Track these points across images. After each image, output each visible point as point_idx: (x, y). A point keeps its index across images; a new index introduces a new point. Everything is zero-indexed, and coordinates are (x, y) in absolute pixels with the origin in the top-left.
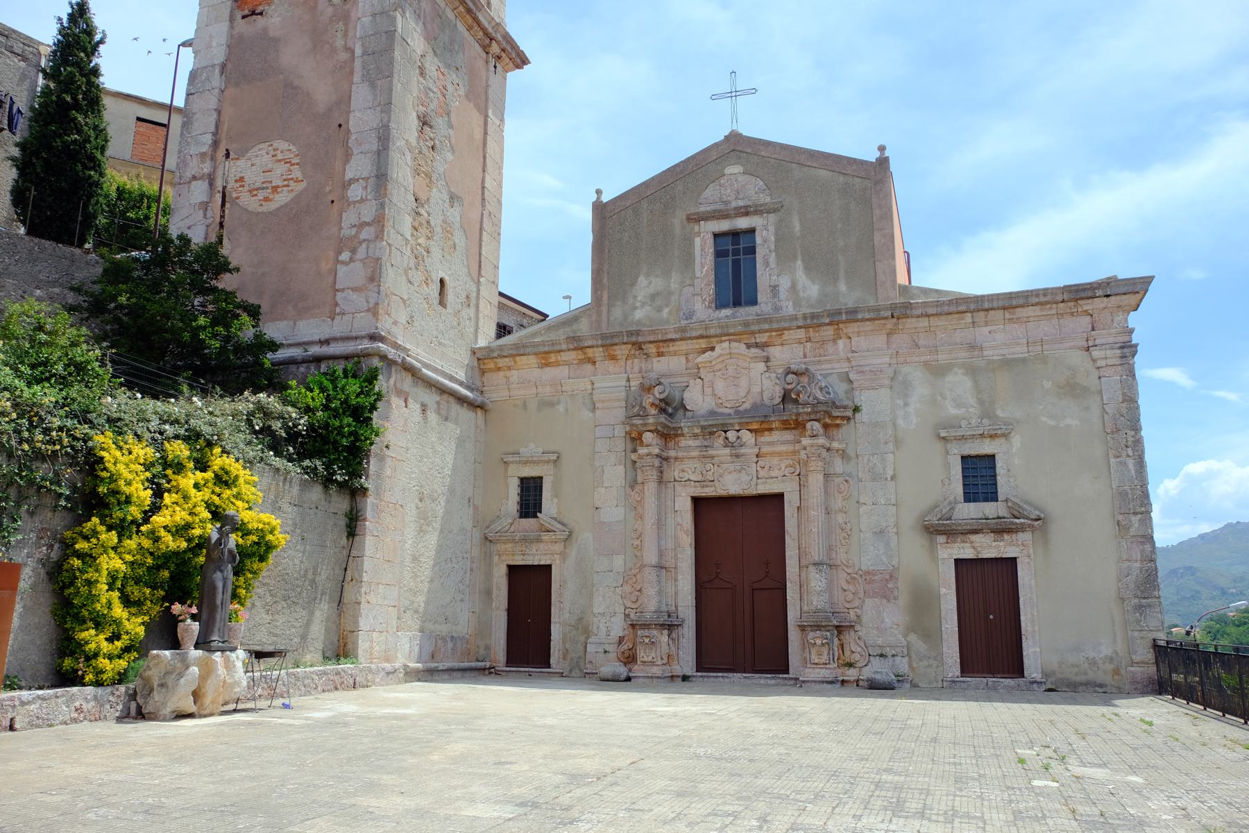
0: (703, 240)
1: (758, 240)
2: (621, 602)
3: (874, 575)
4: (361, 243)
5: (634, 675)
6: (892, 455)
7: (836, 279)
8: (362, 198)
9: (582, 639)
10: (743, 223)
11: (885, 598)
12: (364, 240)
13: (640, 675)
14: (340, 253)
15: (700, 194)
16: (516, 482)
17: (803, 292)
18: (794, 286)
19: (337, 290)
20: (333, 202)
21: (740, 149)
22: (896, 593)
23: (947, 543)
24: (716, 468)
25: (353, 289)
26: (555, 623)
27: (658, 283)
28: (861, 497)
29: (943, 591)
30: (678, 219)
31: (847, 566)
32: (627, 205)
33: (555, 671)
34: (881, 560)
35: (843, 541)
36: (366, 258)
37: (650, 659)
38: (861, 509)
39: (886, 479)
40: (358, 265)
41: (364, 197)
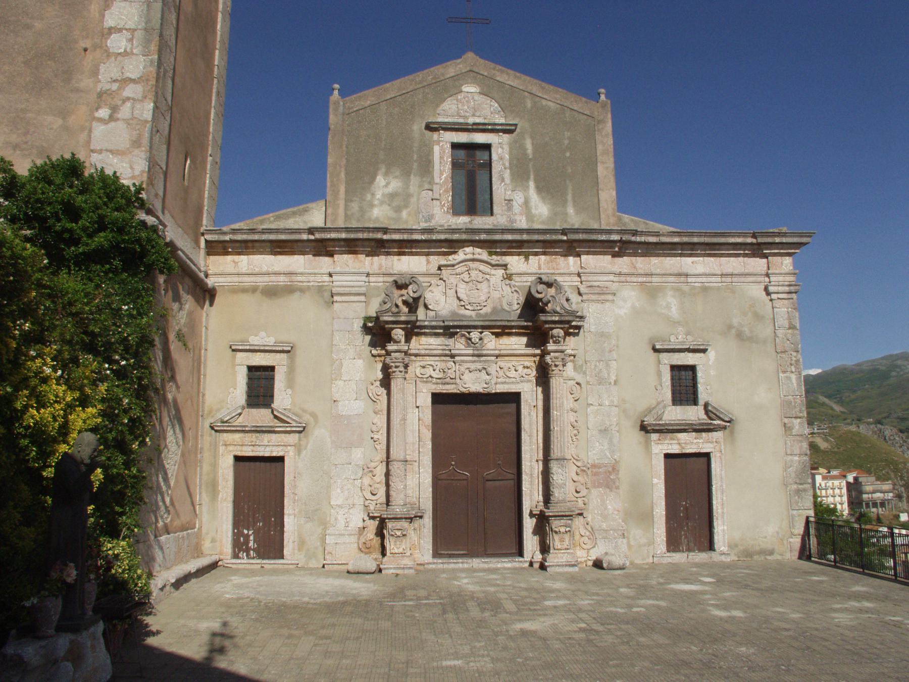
0: (442, 150)
1: (494, 157)
2: (360, 494)
3: (600, 468)
4: (124, 101)
5: (386, 566)
6: (614, 362)
7: (564, 203)
8: (125, 51)
9: (319, 530)
10: (480, 138)
11: (608, 488)
12: (128, 99)
13: (391, 566)
14: (97, 109)
15: (438, 106)
16: (244, 370)
17: (536, 209)
18: (527, 202)
19: (92, 151)
20: (86, 50)
21: (477, 71)
22: (617, 484)
23: (659, 440)
24: (457, 367)
25: (111, 151)
26: (289, 515)
27: (395, 185)
28: (589, 399)
29: (655, 481)
30: (418, 127)
31: (577, 460)
32: (366, 105)
33: (290, 562)
34: (605, 454)
35: (574, 438)
36: (132, 119)
37: (401, 550)
38: (588, 410)
39: (610, 383)
40: (120, 125)
41: (128, 50)
